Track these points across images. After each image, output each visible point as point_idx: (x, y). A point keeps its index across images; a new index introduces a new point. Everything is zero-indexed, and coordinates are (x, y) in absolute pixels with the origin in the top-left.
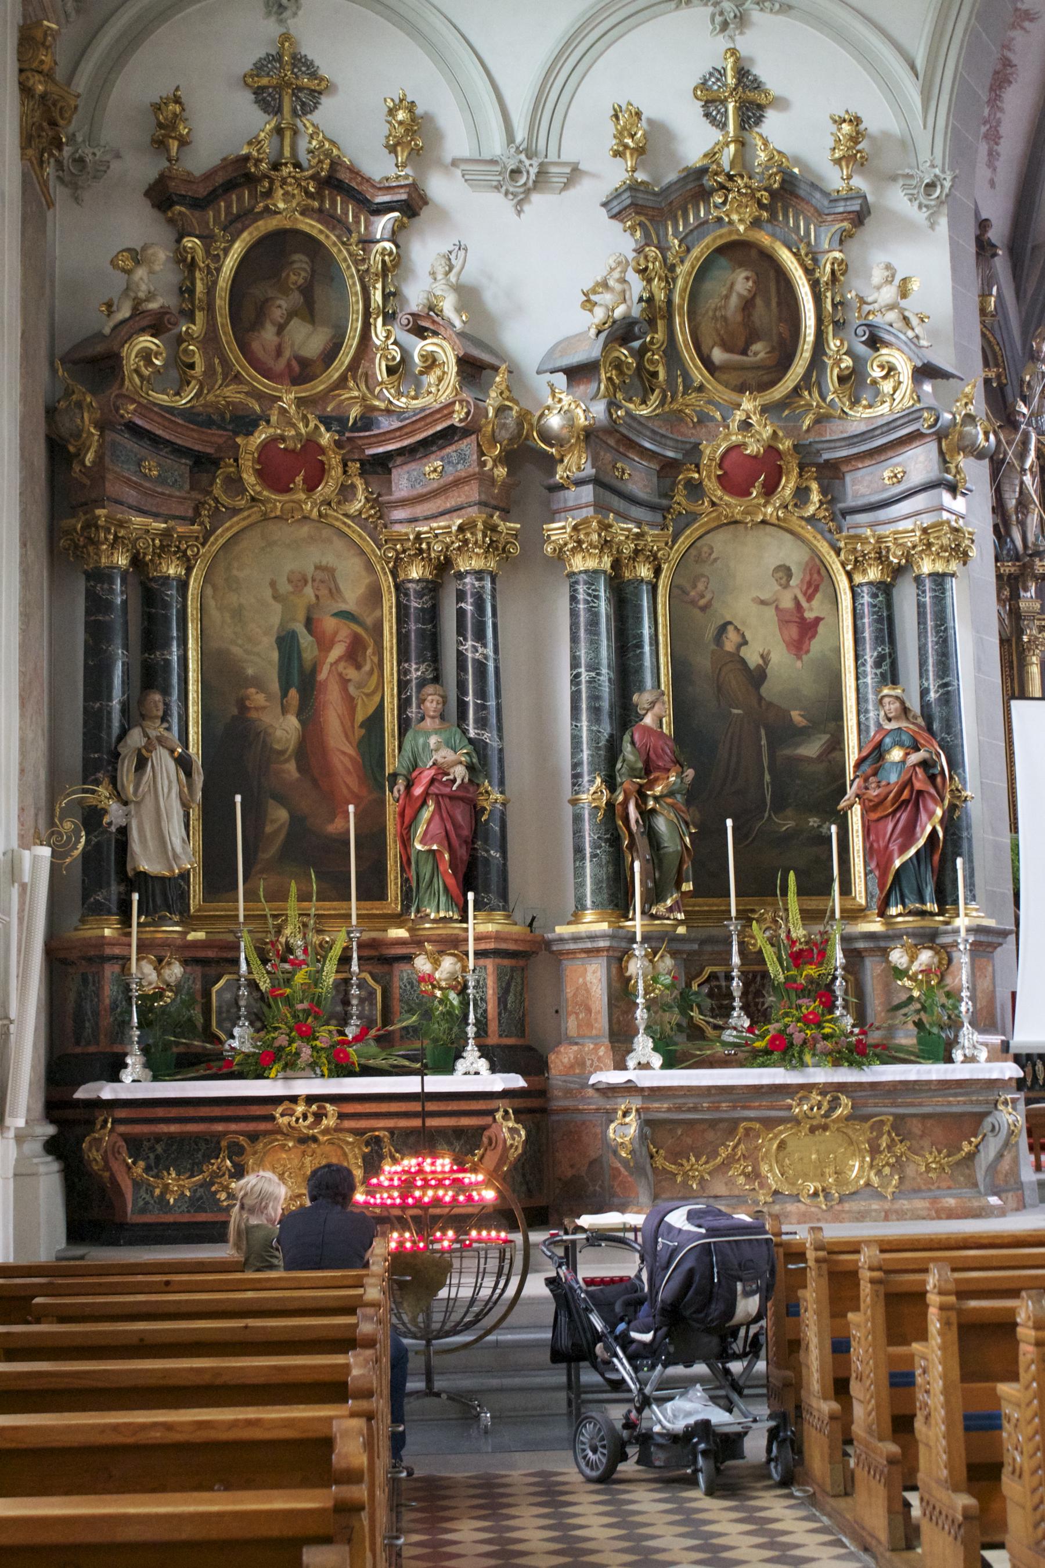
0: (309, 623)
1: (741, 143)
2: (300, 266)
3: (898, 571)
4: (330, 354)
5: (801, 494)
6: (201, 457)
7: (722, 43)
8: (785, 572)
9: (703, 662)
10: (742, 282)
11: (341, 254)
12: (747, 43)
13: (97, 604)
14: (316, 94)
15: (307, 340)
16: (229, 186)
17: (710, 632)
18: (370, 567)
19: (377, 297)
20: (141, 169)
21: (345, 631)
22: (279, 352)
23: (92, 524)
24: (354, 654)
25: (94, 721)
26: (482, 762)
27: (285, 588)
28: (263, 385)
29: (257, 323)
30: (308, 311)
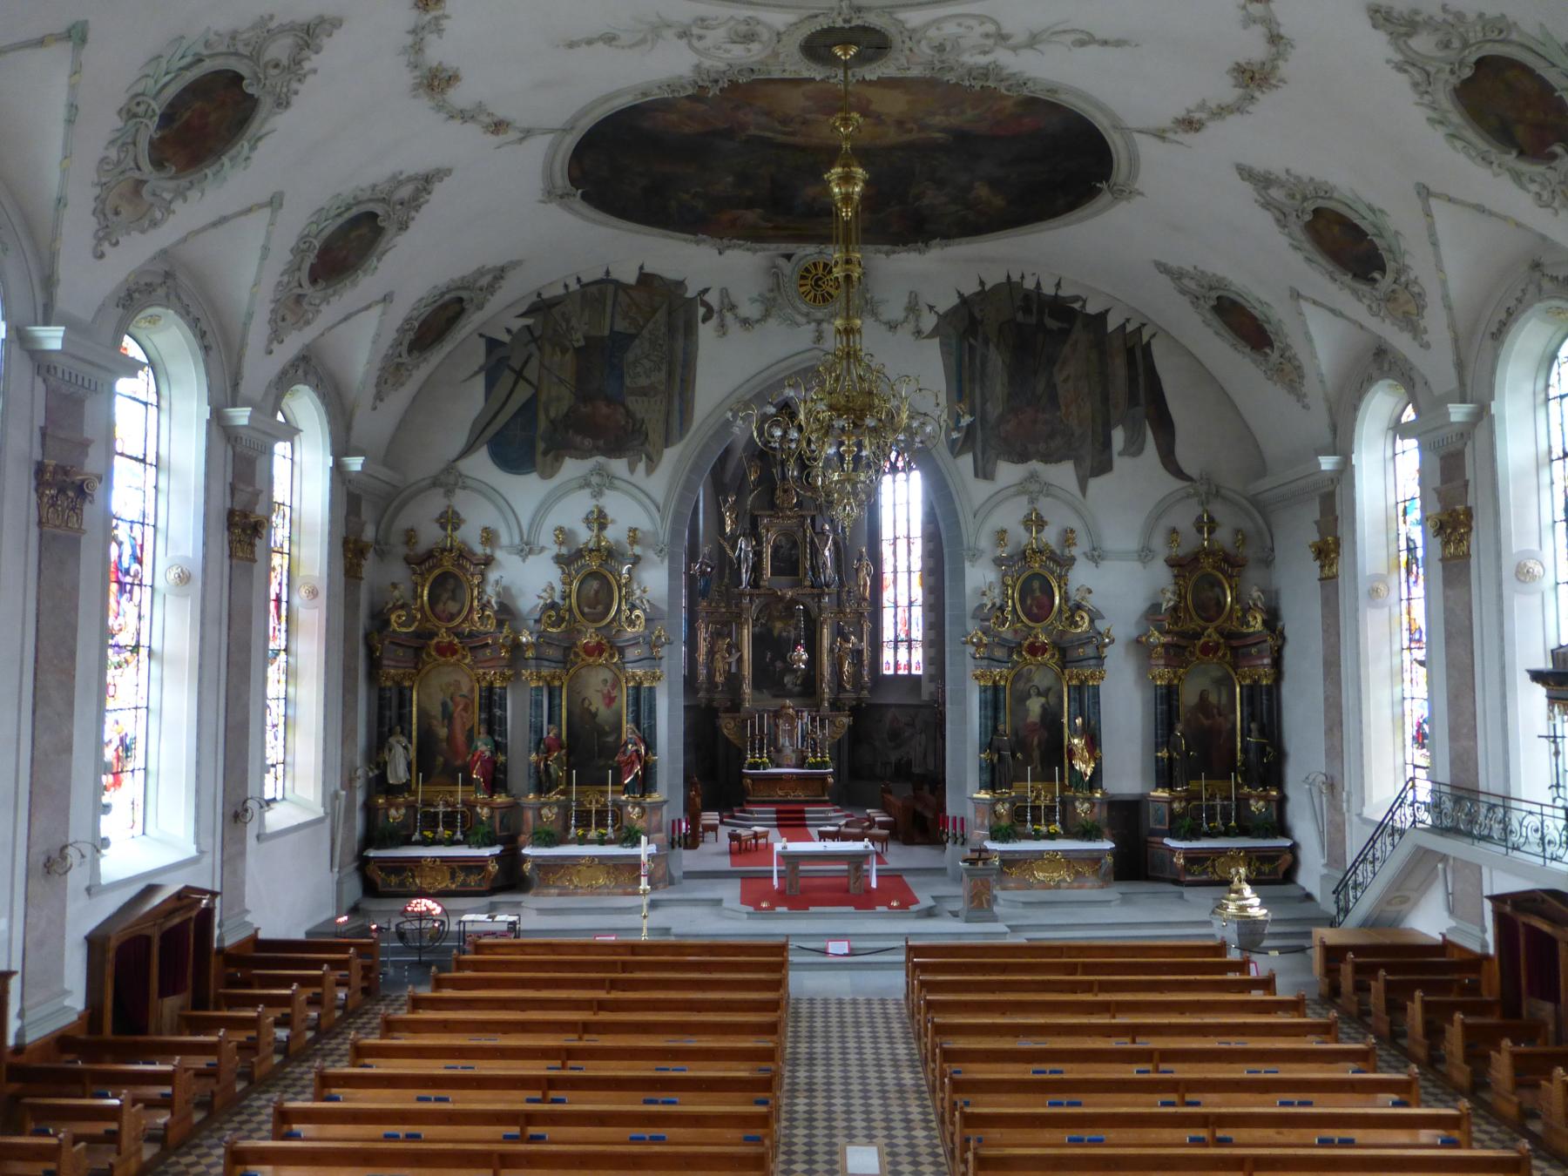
1: (598, 536)
2: (451, 584)
4: (460, 612)
5: (612, 656)
6: (419, 645)
7: (594, 502)
8: (605, 681)
12: (603, 502)
13: (381, 698)
15: (453, 607)
20: (402, 550)
21: (461, 703)
24: (465, 709)
26: (499, 747)
28: (438, 623)
30: (453, 598)
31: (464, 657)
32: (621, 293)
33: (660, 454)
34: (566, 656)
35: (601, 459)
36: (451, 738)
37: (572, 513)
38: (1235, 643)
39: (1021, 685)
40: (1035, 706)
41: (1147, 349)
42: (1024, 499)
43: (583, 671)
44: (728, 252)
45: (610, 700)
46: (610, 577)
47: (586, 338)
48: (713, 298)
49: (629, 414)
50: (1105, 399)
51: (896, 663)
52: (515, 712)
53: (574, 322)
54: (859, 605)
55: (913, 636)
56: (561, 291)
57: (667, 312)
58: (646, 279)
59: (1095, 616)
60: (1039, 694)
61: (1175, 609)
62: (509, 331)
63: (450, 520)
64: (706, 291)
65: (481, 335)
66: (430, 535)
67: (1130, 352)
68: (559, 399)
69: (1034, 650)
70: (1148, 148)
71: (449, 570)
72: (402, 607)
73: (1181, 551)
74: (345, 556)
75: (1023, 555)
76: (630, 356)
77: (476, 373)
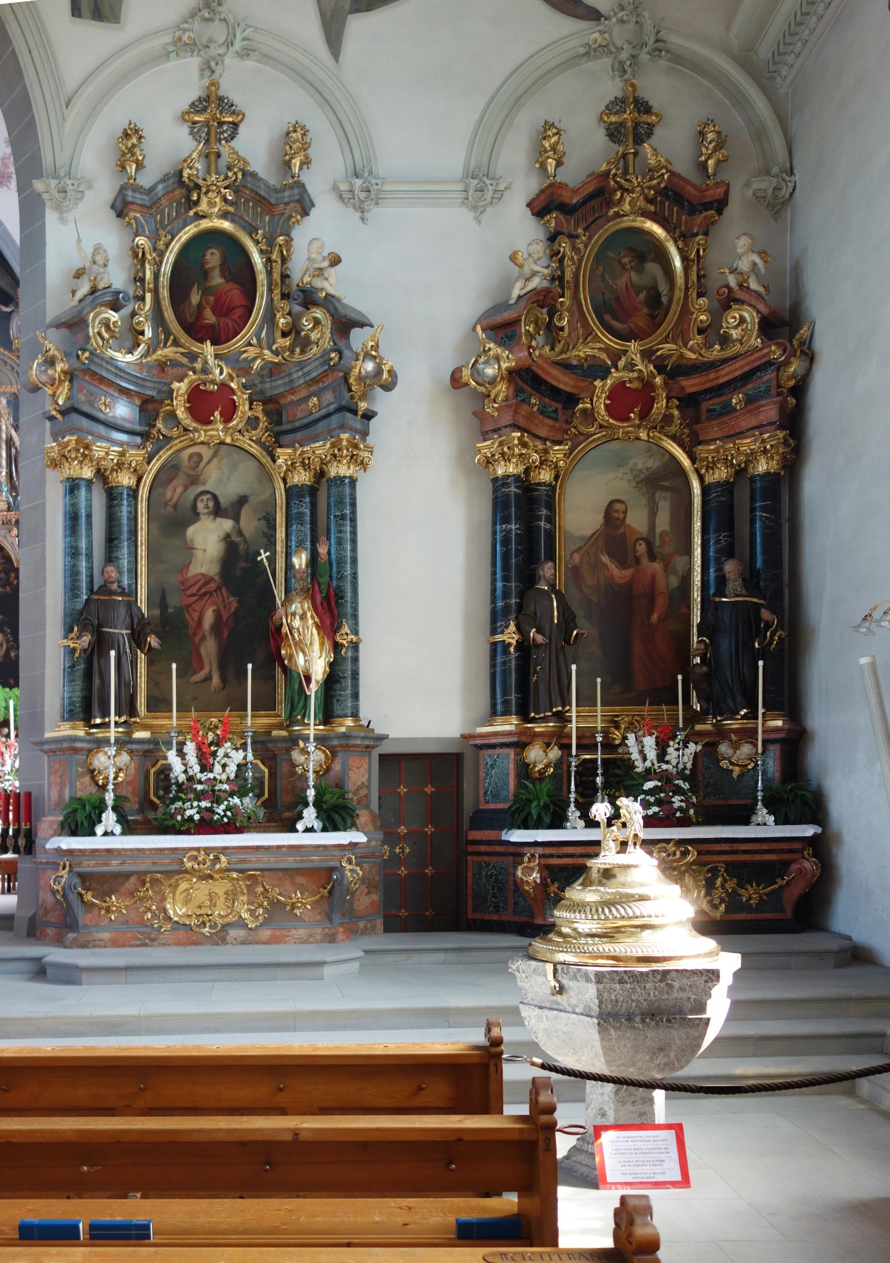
38: (691, 385)
39: (174, 492)
40: (207, 539)
42: (193, 63)
59: (345, 324)
60: (218, 511)
61: (543, 300)
69: (203, 404)
75: (184, 191)
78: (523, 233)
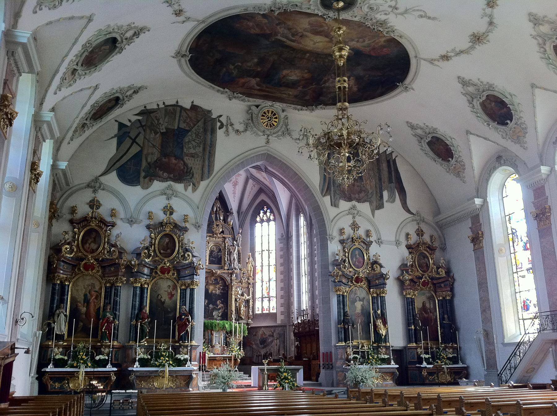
0: (89, 293)
3: (187, 287)
5: (173, 274)
7: (167, 202)
9: (155, 301)
10: (167, 240)
11: (101, 233)
13: (54, 289)
14: (99, 207)
15: (94, 246)
16: (83, 221)
17: (156, 296)
18: (100, 283)
19: (106, 240)
20: (69, 217)
22: (89, 248)
23: (54, 276)
25: (51, 308)
26: (115, 316)
27: (86, 286)
29: (86, 243)
30: (94, 242)
31: (98, 271)
32: (183, 111)
33: (199, 183)
34: (151, 273)
35: (172, 183)
36: (88, 313)
37: (156, 206)
38: (435, 282)
39: (352, 296)
41: (394, 161)
42: (351, 216)
43: (160, 282)
44: (234, 100)
45: (171, 295)
46: (175, 237)
47: (166, 129)
48: (223, 119)
49: (185, 164)
50: (380, 179)
51: (263, 307)
52: (125, 298)
53: (161, 121)
54: (248, 279)
55: (271, 295)
56: (156, 107)
57: (203, 124)
58: (194, 108)
60: (360, 300)
62: (130, 121)
63: (94, 204)
64: (221, 116)
65: (116, 121)
66: (83, 210)
67: (388, 162)
68: (153, 154)
70: (425, 67)
71: (93, 229)
72: (68, 244)
73: (411, 242)
74: (50, 211)
76: (186, 140)
77: (112, 138)
78: (406, 252)
